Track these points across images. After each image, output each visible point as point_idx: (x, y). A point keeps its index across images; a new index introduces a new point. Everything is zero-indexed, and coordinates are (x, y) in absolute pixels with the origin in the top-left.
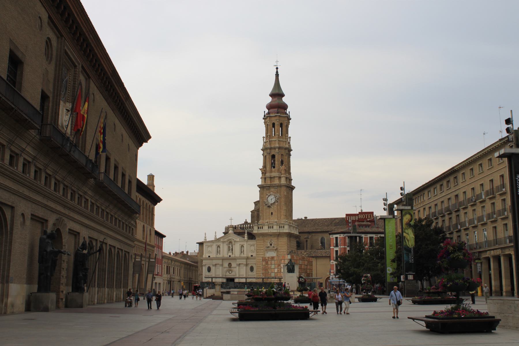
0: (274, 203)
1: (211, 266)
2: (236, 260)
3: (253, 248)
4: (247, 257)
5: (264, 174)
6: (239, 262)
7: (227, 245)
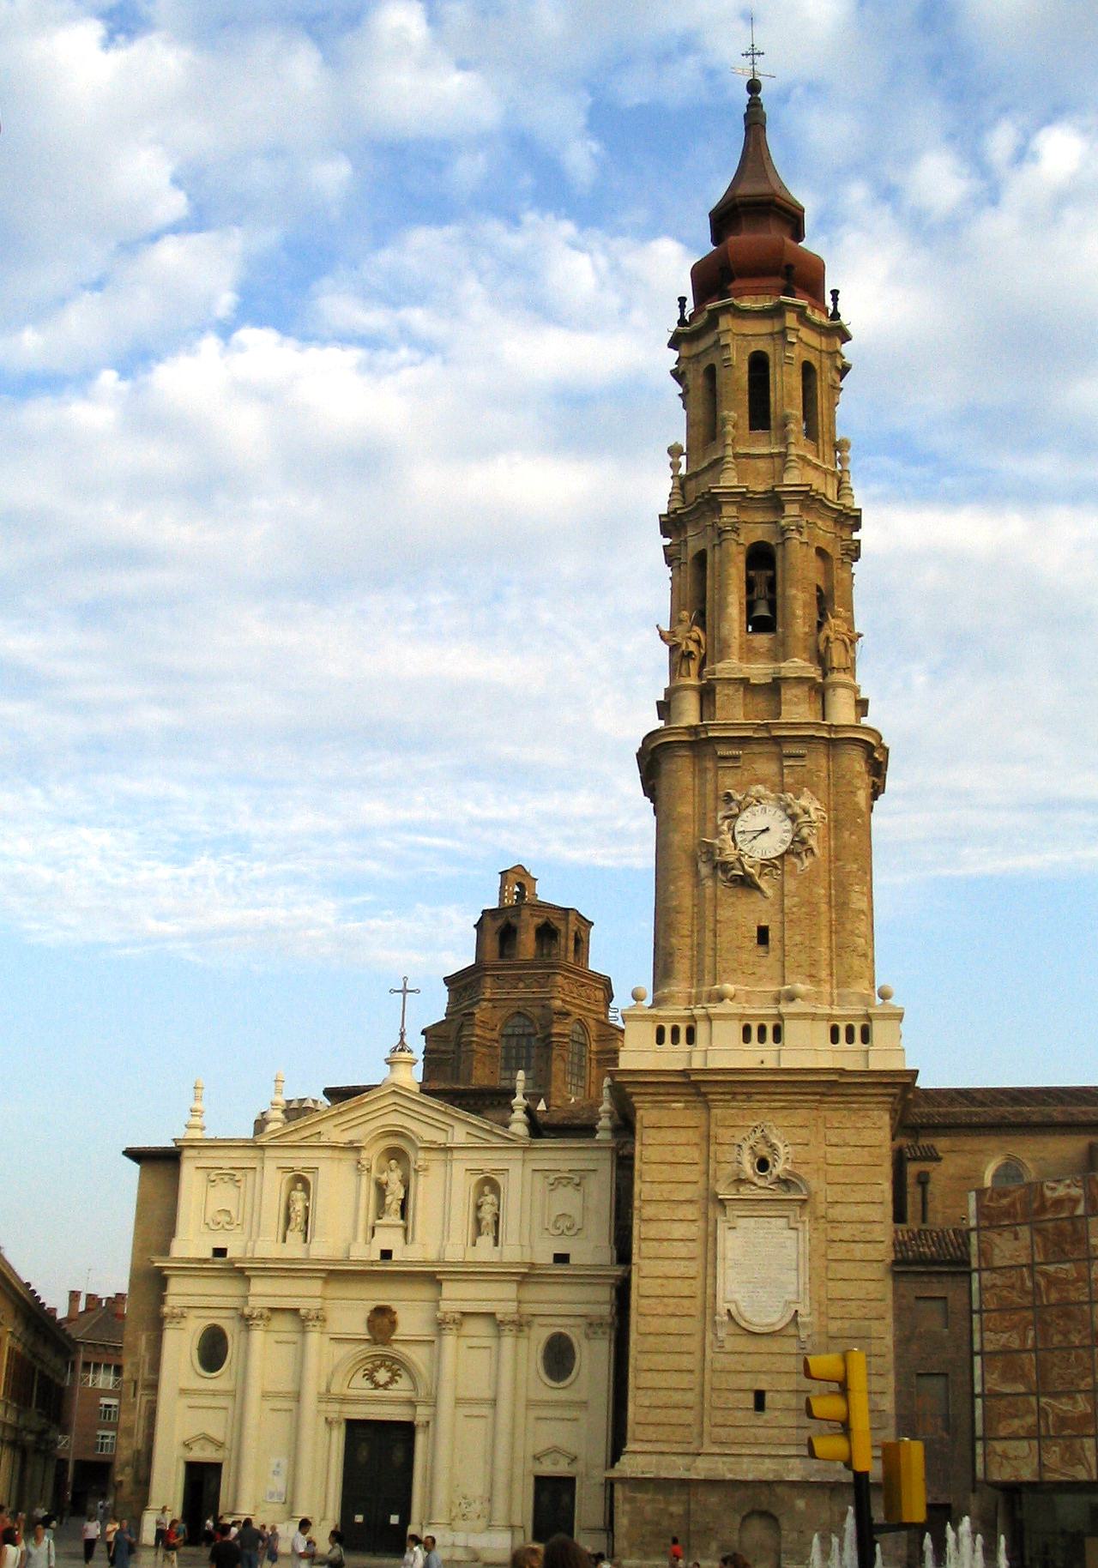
0: (781, 857)
1: (230, 1328)
2: (439, 1283)
3: (567, 1201)
4: (532, 1265)
5: (694, 666)
6: (457, 1295)
7: (369, 1170)
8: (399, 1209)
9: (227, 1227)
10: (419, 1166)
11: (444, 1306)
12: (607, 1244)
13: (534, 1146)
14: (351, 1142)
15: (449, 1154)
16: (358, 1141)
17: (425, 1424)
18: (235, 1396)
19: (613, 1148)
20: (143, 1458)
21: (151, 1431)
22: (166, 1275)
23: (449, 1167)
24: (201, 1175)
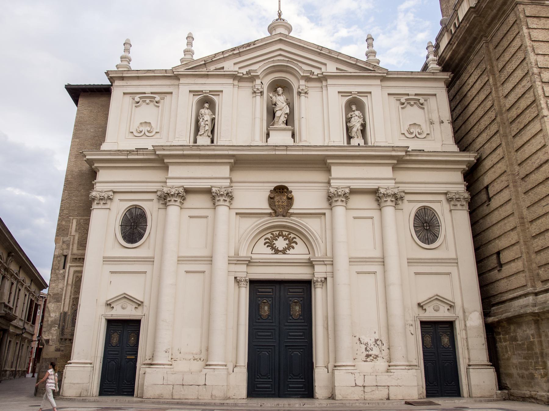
7: (262, 93)
8: (285, 122)
9: (147, 134)
10: (302, 90)
11: (334, 183)
12: (452, 143)
13: (389, 76)
14: (248, 73)
15: (324, 83)
16: (255, 71)
17: (323, 279)
18: (153, 261)
19: (445, 81)
20: (69, 319)
21: (77, 296)
22: (97, 167)
23: (324, 92)
24: (128, 98)
